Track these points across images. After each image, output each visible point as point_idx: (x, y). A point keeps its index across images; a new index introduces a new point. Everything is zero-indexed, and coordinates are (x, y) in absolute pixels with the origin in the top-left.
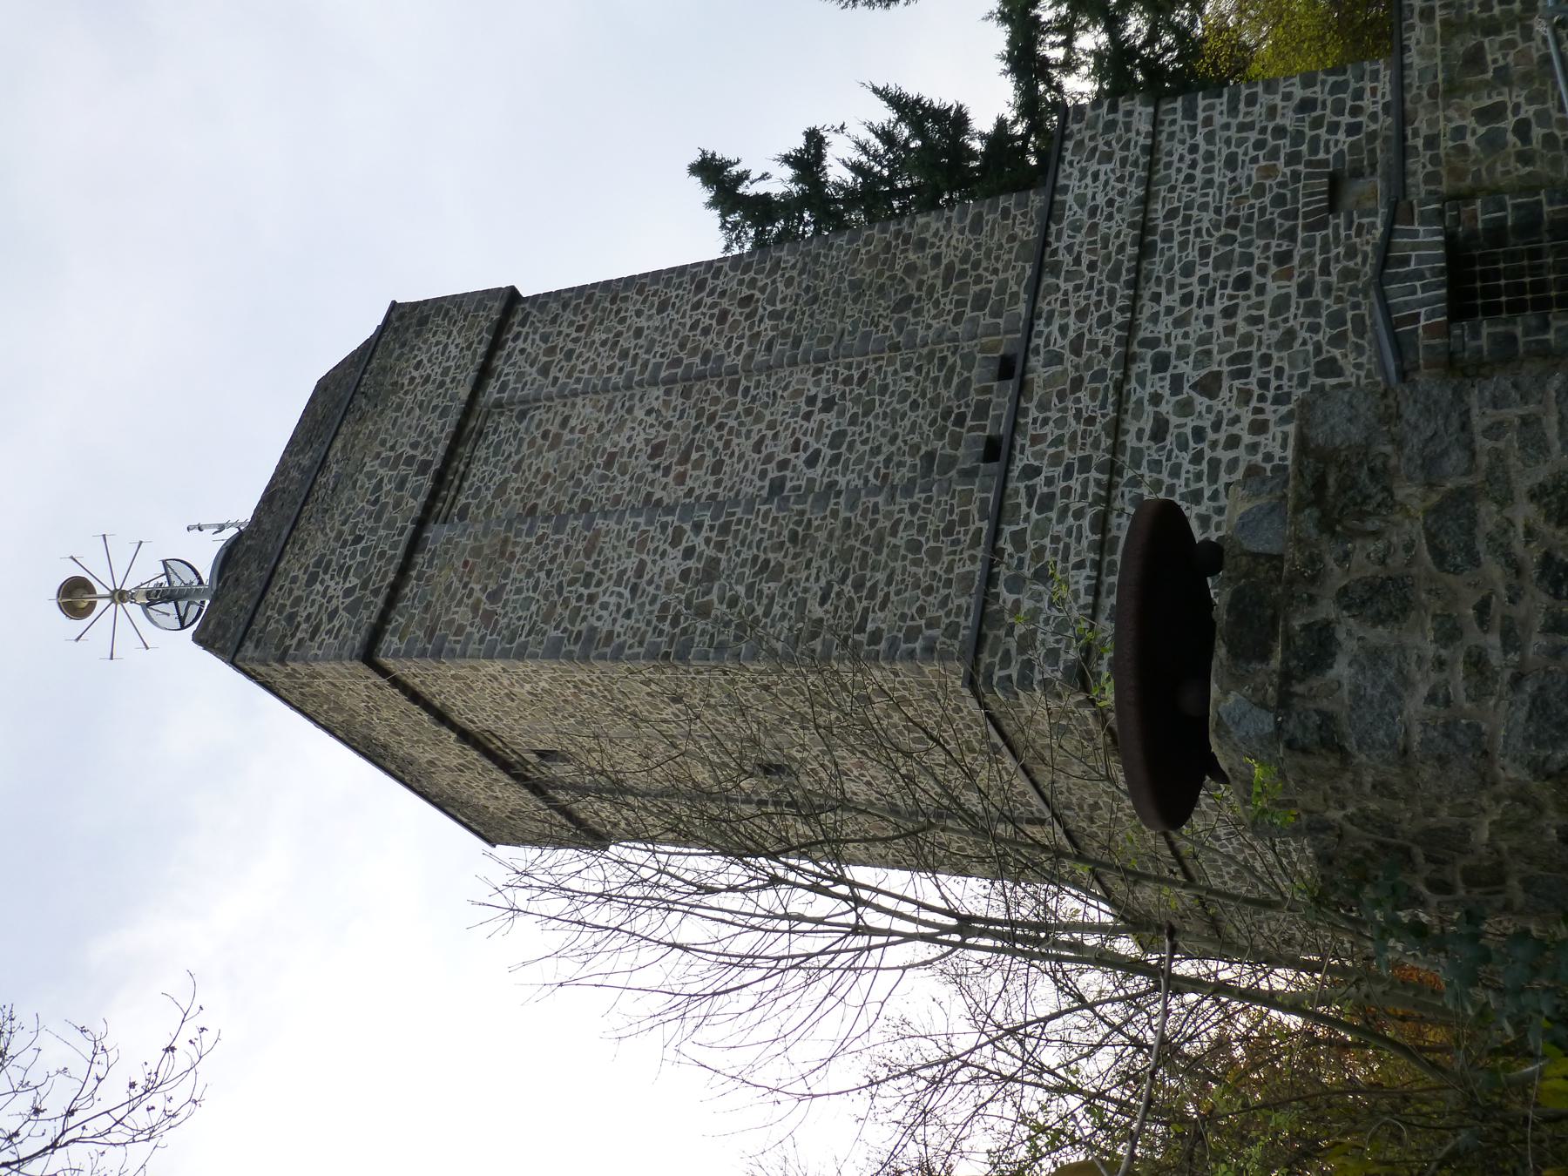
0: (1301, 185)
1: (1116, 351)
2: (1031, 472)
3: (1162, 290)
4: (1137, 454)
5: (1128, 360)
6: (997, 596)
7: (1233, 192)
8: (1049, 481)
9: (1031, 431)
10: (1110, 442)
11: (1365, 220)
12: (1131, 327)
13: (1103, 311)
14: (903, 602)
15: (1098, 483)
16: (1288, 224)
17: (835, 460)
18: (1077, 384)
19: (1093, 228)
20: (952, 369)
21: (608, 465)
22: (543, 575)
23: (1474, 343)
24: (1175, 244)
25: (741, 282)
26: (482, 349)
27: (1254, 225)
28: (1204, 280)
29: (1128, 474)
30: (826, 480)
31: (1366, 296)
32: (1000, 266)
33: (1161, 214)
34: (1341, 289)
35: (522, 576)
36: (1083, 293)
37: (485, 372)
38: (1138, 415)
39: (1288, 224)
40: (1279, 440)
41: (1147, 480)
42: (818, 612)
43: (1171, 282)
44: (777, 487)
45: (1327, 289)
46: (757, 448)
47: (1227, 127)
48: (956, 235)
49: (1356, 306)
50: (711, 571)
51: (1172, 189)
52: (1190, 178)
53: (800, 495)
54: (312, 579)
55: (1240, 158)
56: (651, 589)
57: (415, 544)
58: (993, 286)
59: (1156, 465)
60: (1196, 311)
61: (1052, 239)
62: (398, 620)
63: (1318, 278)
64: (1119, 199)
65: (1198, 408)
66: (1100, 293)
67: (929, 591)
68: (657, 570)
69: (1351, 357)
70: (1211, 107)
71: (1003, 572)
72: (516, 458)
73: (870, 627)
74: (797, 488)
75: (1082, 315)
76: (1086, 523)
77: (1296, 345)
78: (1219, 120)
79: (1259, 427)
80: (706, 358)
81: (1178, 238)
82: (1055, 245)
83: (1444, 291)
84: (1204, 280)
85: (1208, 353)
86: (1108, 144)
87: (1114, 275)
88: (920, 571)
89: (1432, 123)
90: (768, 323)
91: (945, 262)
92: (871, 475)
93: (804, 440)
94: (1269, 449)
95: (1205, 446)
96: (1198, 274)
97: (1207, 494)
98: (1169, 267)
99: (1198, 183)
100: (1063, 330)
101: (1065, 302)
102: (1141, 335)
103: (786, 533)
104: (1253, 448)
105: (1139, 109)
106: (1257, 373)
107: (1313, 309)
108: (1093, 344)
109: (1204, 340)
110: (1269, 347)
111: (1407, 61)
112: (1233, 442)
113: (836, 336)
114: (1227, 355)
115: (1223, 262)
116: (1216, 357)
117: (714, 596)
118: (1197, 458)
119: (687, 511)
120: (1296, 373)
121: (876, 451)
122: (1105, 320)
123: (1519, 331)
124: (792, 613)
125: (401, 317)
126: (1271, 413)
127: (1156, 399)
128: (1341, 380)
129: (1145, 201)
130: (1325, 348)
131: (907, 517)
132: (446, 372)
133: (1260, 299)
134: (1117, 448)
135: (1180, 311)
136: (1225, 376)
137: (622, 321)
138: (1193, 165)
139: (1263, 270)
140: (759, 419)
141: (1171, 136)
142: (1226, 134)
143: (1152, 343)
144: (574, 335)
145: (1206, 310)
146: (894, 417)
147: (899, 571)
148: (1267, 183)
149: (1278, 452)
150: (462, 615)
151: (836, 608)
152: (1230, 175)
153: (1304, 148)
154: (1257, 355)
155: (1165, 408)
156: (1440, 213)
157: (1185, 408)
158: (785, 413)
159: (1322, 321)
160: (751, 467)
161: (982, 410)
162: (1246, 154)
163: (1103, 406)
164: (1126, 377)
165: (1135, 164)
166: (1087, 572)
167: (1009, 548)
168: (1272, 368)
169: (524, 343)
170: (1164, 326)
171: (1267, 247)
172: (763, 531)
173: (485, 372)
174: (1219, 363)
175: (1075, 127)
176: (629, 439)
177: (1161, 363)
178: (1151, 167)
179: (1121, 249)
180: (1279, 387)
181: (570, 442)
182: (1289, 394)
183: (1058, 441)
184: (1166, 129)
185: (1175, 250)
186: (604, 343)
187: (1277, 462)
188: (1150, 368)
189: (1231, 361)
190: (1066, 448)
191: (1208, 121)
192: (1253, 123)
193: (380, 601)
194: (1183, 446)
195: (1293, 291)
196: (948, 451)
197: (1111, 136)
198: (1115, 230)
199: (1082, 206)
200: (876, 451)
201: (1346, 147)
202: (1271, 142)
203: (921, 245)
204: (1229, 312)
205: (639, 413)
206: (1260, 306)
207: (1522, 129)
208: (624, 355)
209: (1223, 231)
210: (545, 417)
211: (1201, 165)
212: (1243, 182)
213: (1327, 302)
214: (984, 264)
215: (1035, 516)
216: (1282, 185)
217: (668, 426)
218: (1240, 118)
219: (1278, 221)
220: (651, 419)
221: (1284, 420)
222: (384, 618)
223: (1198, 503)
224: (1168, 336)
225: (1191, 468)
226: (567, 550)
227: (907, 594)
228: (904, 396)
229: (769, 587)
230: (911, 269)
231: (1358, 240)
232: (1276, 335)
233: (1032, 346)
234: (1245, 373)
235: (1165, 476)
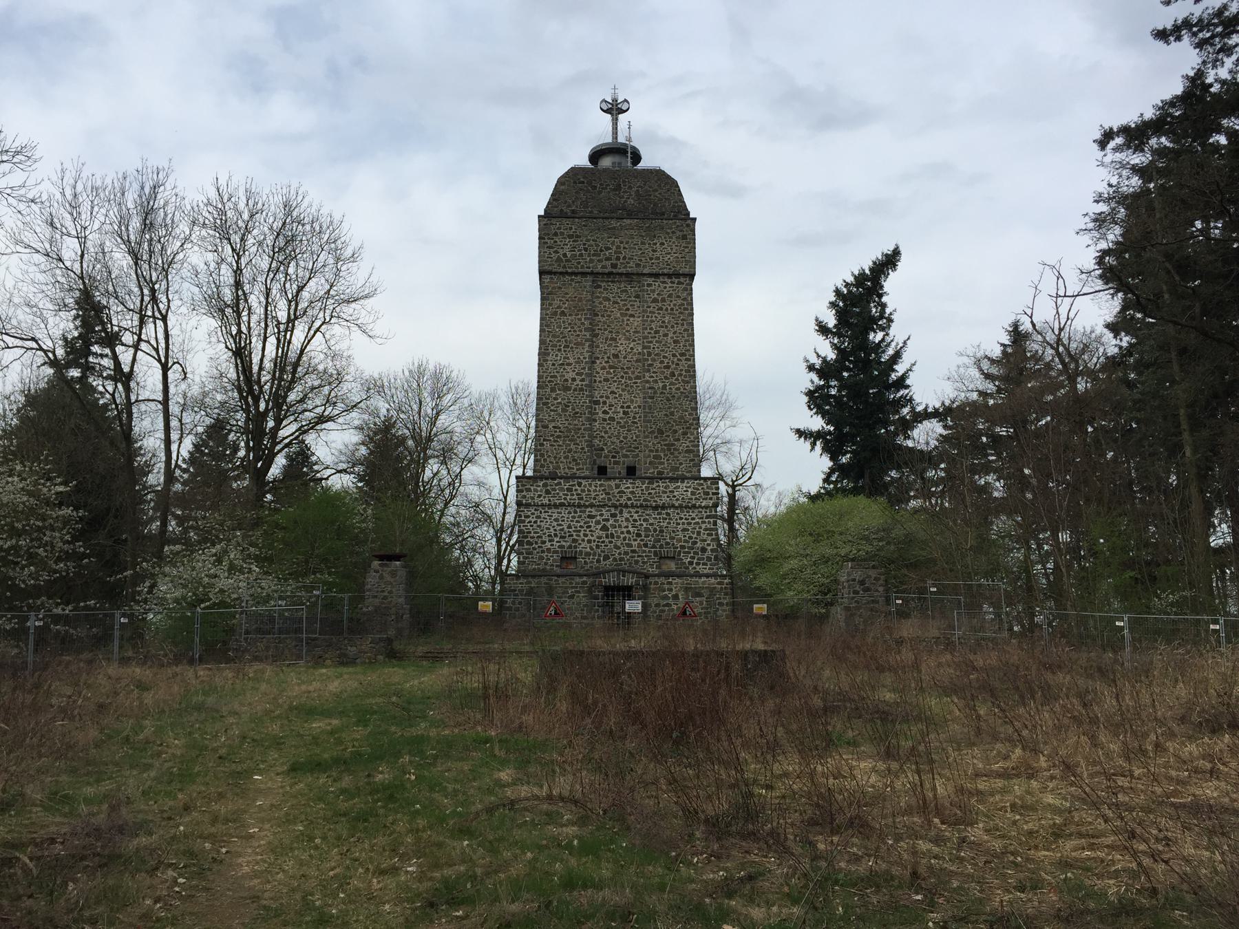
5: (616, 507)
12: (626, 506)
17: (605, 420)
18: (607, 494)
21: (612, 339)
26: (665, 271)
37: (656, 276)
44: (597, 403)
46: (613, 392)
50: (568, 389)
54: (570, 236)
57: (584, 274)
62: (555, 278)
71: (549, 482)
75: (632, 493)
78: (703, 526)
79: (589, 541)
80: (651, 365)
87: (645, 500)
90: (661, 385)
107: (626, 553)
109: (620, 526)
112: (586, 535)
115: (647, 529)
119: (590, 375)
121: (606, 432)
122: (629, 499)
125: (688, 225)
127: (601, 515)
129: (673, 506)
132: (658, 258)
140: (623, 390)
143: (621, 512)
146: (618, 437)
150: (557, 303)
157: (598, 523)
161: (616, 463)
169: (669, 286)
170: (626, 515)
173: (656, 276)
174: (611, 530)
177: (614, 515)
178: (686, 507)
200: (606, 432)
203: (685, 434)
204: (628, 532)
207: (668, 605)
208: (657, 332)
221: (591, 548)
222: (555, 273)
228: (625, 438)
230: (675, 431)
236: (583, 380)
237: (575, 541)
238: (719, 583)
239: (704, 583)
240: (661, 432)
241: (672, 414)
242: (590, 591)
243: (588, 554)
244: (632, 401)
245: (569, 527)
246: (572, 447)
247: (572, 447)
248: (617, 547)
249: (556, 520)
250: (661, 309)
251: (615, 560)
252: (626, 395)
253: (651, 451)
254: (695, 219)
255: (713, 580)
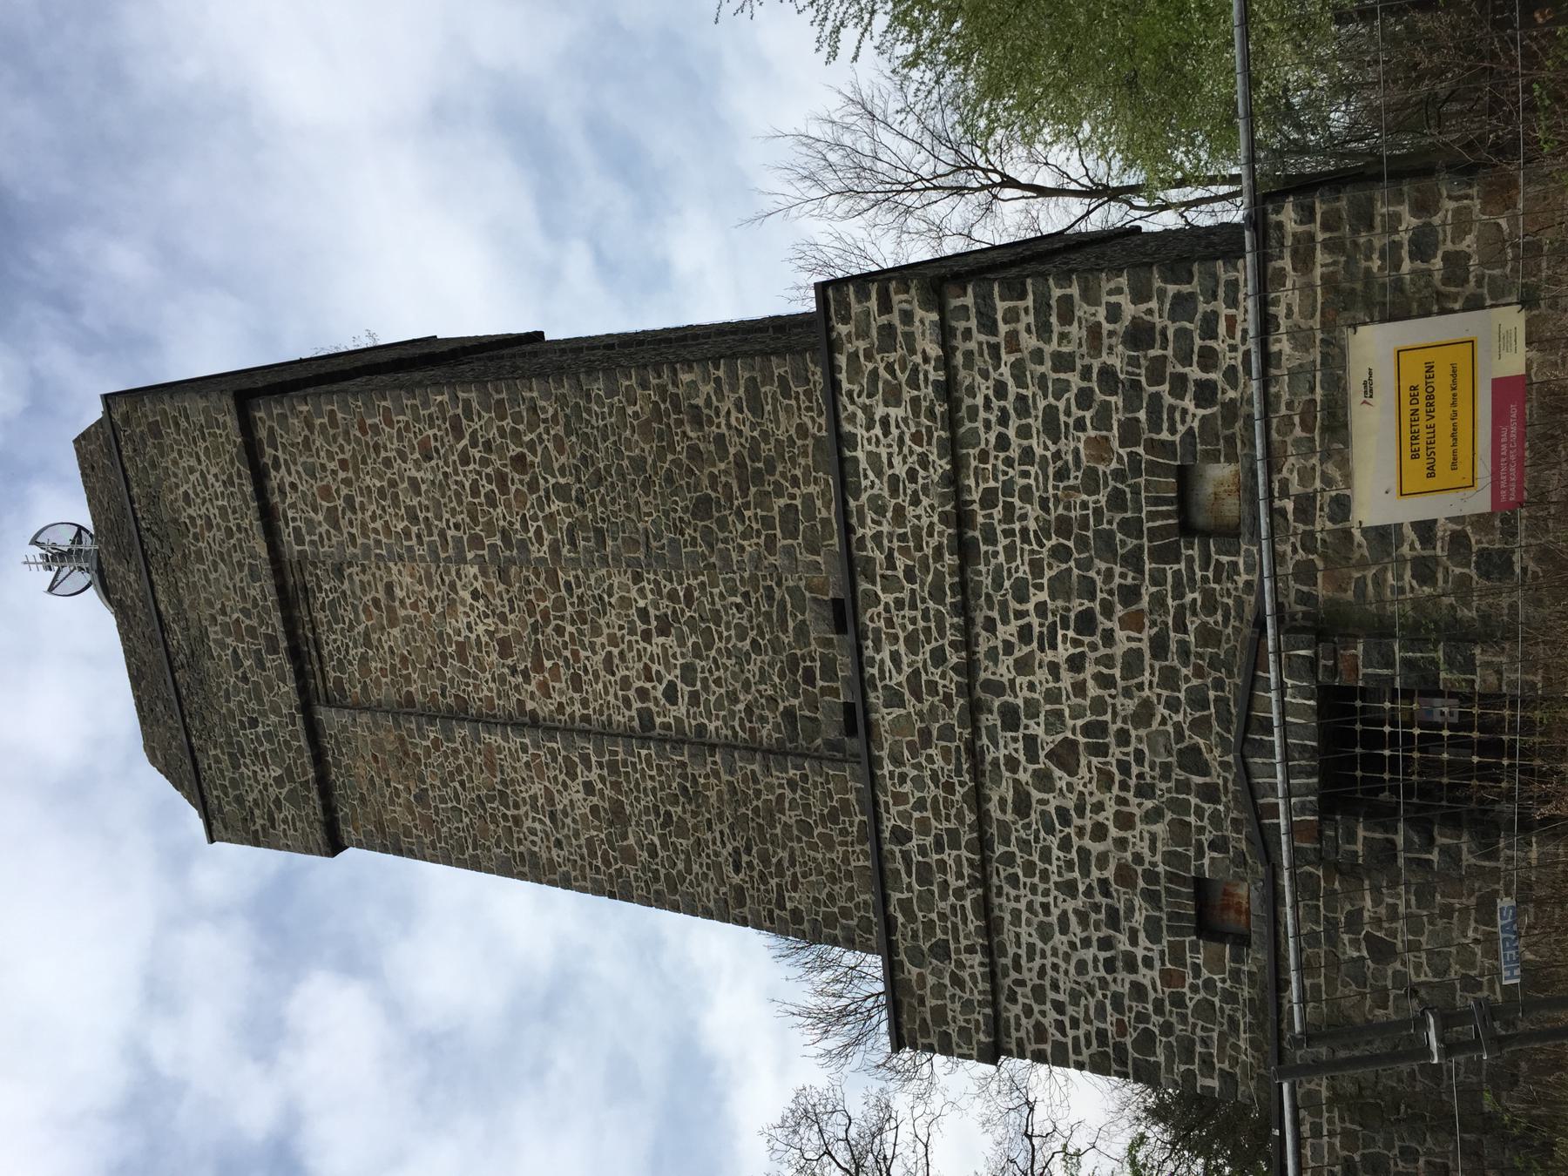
0: (1142, 481)
1: (959, 702)
2: (901, 836)
3: (995, 614)
4: (1003, 825)
5: (974, 709)
6: (901, 963)
7: (1061, 475)
8: (922, 850)
9: (890, 788)
10: (973, 817)
11: (1225, 559)
12: (969, 669)
13: (934, 644)
14: (812, 884)
15: (971, 862)
16: (1132, 543)
17: (694, 699)
19: (899, 511)
20: (782, 603)
22: (457, 785)
23: (1348, 847)
24: (1000, 548)
25: (501, 430)
26: (249, 489)
27: (1090, 534)
28: (1041, 609)
29: (1000, 850)
30: (693, 723)
31: (1230, 674)
32: (798, 472)
33: (976, 496)
34: (1200, 656)
35: (437, 783)
36: (907, 612)
37: (268, 517)
38: (997, 780)
39: (1132, 543)
40: (1146, 843)
41: (1019, 861)
42: (736, 880)
43: (1004, 605)
44: (646, 718)
45: (1184, 652)
47: (1038, 356)
48: (734, 414)
49: (1219, 684)
51: (984, 457)
52: (1003, 443)
53: (675, 739)
55: (1063, 418)
56: (568, 821)
58: (798, 502)
59: (1024, 845)
60: (1038, 655)
61: (854, 521)
62: (344, 811)
63: (1172, 634)
64: (922, 473)
65: (1058, 784)
66: (926, 618)
67: (833, 879)
68: (566, 802)
69: (1217, 752)
70: (1012, 316)
72: (361, 628)
73: (789, 905)
74: (667, 726)
75: (913, 643)
76: (968, 904)
77: (1155, 725)
78: (1029, 342)
79: (1125, 821)
81: (1003, 541)
82: (860, 532)
83: (1315, 780)
84: (1041, 609)
85: (1059, 714)
86: (890, 368)
87: (937, 593)
88: (820, 856)
89: (1306, 475)
90: (557, 505)
91: (732, 451)
92: (736, 724)
93: (655, 667)
94: (1137, 849)
95: (1072, 831)
96: (1033, 601)
97: (1081, 888)
98: (998, 585)
99: (1014, 453)
100: (895, 657)
101: (890, 623)
102: (983, 676)
103: (674, 785)
104: (1121, 843)
105: (919, 313)
106: (1116, 752)
107: (1169, 679)
108: (932, 686)
109: (1053, 696)
110: (1125, 721)
111: (1275, 348)
113: (642, 539)
114: (1080, 722)
115: (1059, 587)
116: (1070, 723)
117: (631, 841)
118: (1065, 845)
120: (1158, 760)
122: (938, 657)
123: (1400, 840)
124: (711, 874)
126: (1137, 807)
127: (1013, 764)
128: (1208, 780)
129: (953, 481)
130: (1187, 733)
131: (787, 792)
133: (1108, 651)
134: (983, 818)
135: (1021, 651)
136: (1081, 748)
137: (388, 463)
138: (1004, 420)
139: (1108, 610)
141: (968, 355)
142: (1041, 369)
143: (996, 688)
144: (342, 475)
145: (1049, 656)
147: (798, 853)
148: (1101, 468)
149: (1146, 853)
151: (751, 877)
152: (1053, 448)
153: (1142, 415)
154: (1113, 728)
155: (1024, 777)
156: (1312, 663)
157: (1044, 780)
158: (621, 628)
159: (1182, 696)
160: (612, 691)
162: (1068, 413)
163: (959, 772)
164: (976, 732)
165: (931, 414)
166: (978, 958)
167: (901, 919)
168: (1131, 749)
170: (1004, 670)
171: (1109, 575)
172: (652, 778)
173: (268, 517)
174: (1073, 728)
175: (843, 329)
176: (470, 628)
177: (1010, 718)
178: (952, 422)
179: (938, 550)
180: (1141, 776)
181: (408, 619)
182: (1152, 787)
183: (920, 805)
184: (961, 345)
185: (1001, 558)
186: (382, 493)
187: (1147, 866)
188: (999, 723)
189: (1087, 730)
190: (929, 814)
191: (1013, 337)
192: (1071, 355)
193: (314, 794)
194: (1050, 830)
195: (1145, 646)
196: (807, 713)
197: (892, 357)
198: (925, 521)
199: (879, 474)
201: (1196, 424)
202: (1099, 396)
204: (1076, 663)
205: (466, 595)
206: (1108, 661)
209: (1054, 541)
210: (365, 578)
211: (1014, 422)
212: (1070, 458)
213: (1184, 671)
214: (780, 468)
215: (916, 887)
216: (1119, 475)
217: (503, 618)
218: (1054, 345)
219: (1119, 536)
220: (480, 604)
221: (1154, 816)
223: (1074, 897)
224: (1012, 682)
225: (1061, 854)
226: (469, 761)
227: (813, 878)
229: (684, 843)
230: (694, 453)
231: (1217, 587)
232: (1131, 705)
233: (867, 676)
234: (1102, 750)
235: (1035, 858)
236: (586, 760)
237: (1125, 876)
238: (1303, 260)
239: (1301, 338)
240: (703, 507)
241: (639, 464)
242: (1350, 871)
243: (1180, 831)
244: (625, 602)
245: (1069, 888)
246: (790, 817)
247: (790, 817)
248: (1144, 714)
249: (1045, 932)
250: (349, 500)
251: (1200, 726)
252: (611, 620)
253: (771, 540)
254: (107, 398)
255: (1287, 298)
